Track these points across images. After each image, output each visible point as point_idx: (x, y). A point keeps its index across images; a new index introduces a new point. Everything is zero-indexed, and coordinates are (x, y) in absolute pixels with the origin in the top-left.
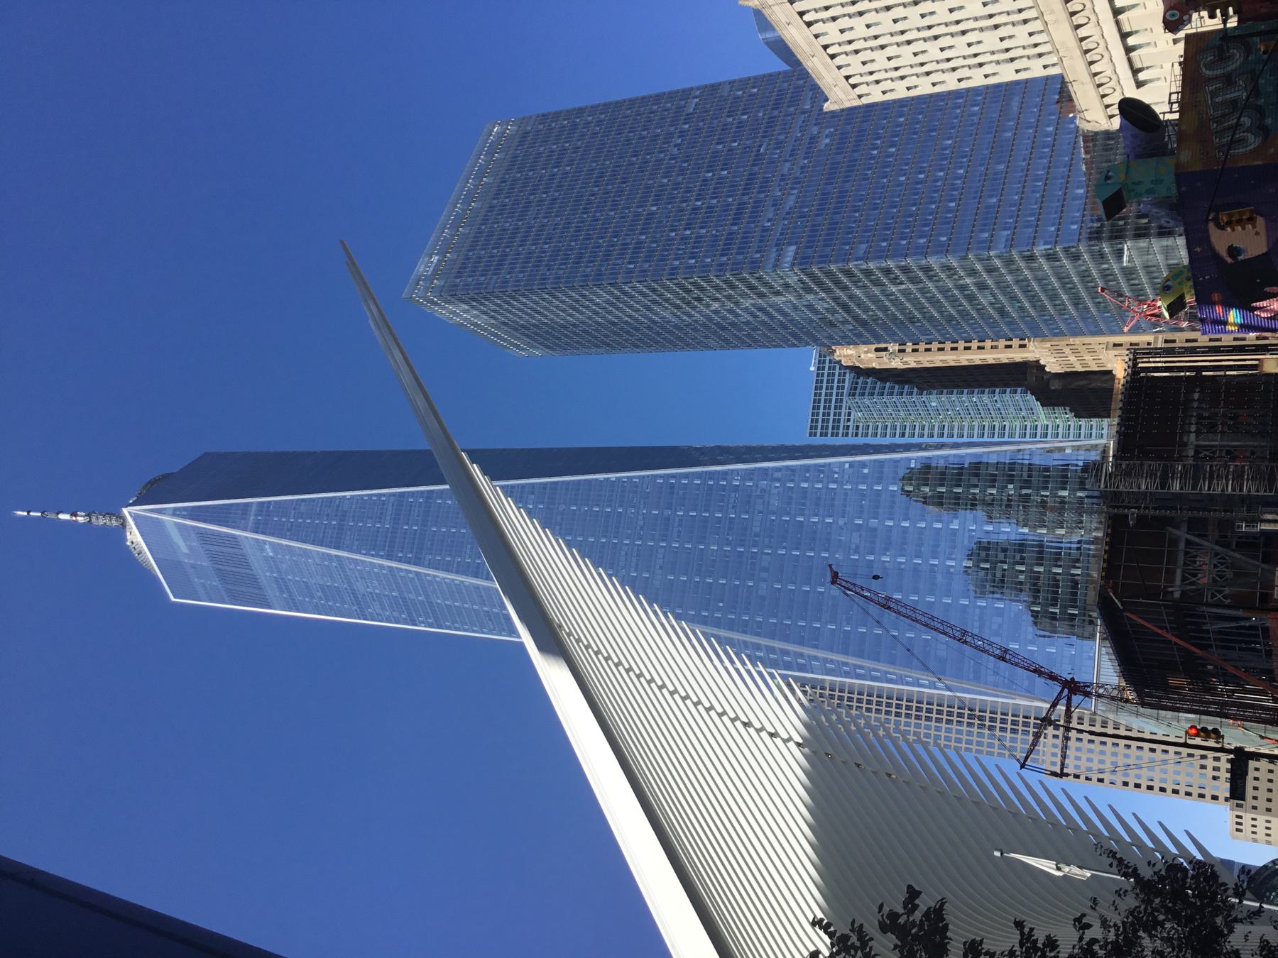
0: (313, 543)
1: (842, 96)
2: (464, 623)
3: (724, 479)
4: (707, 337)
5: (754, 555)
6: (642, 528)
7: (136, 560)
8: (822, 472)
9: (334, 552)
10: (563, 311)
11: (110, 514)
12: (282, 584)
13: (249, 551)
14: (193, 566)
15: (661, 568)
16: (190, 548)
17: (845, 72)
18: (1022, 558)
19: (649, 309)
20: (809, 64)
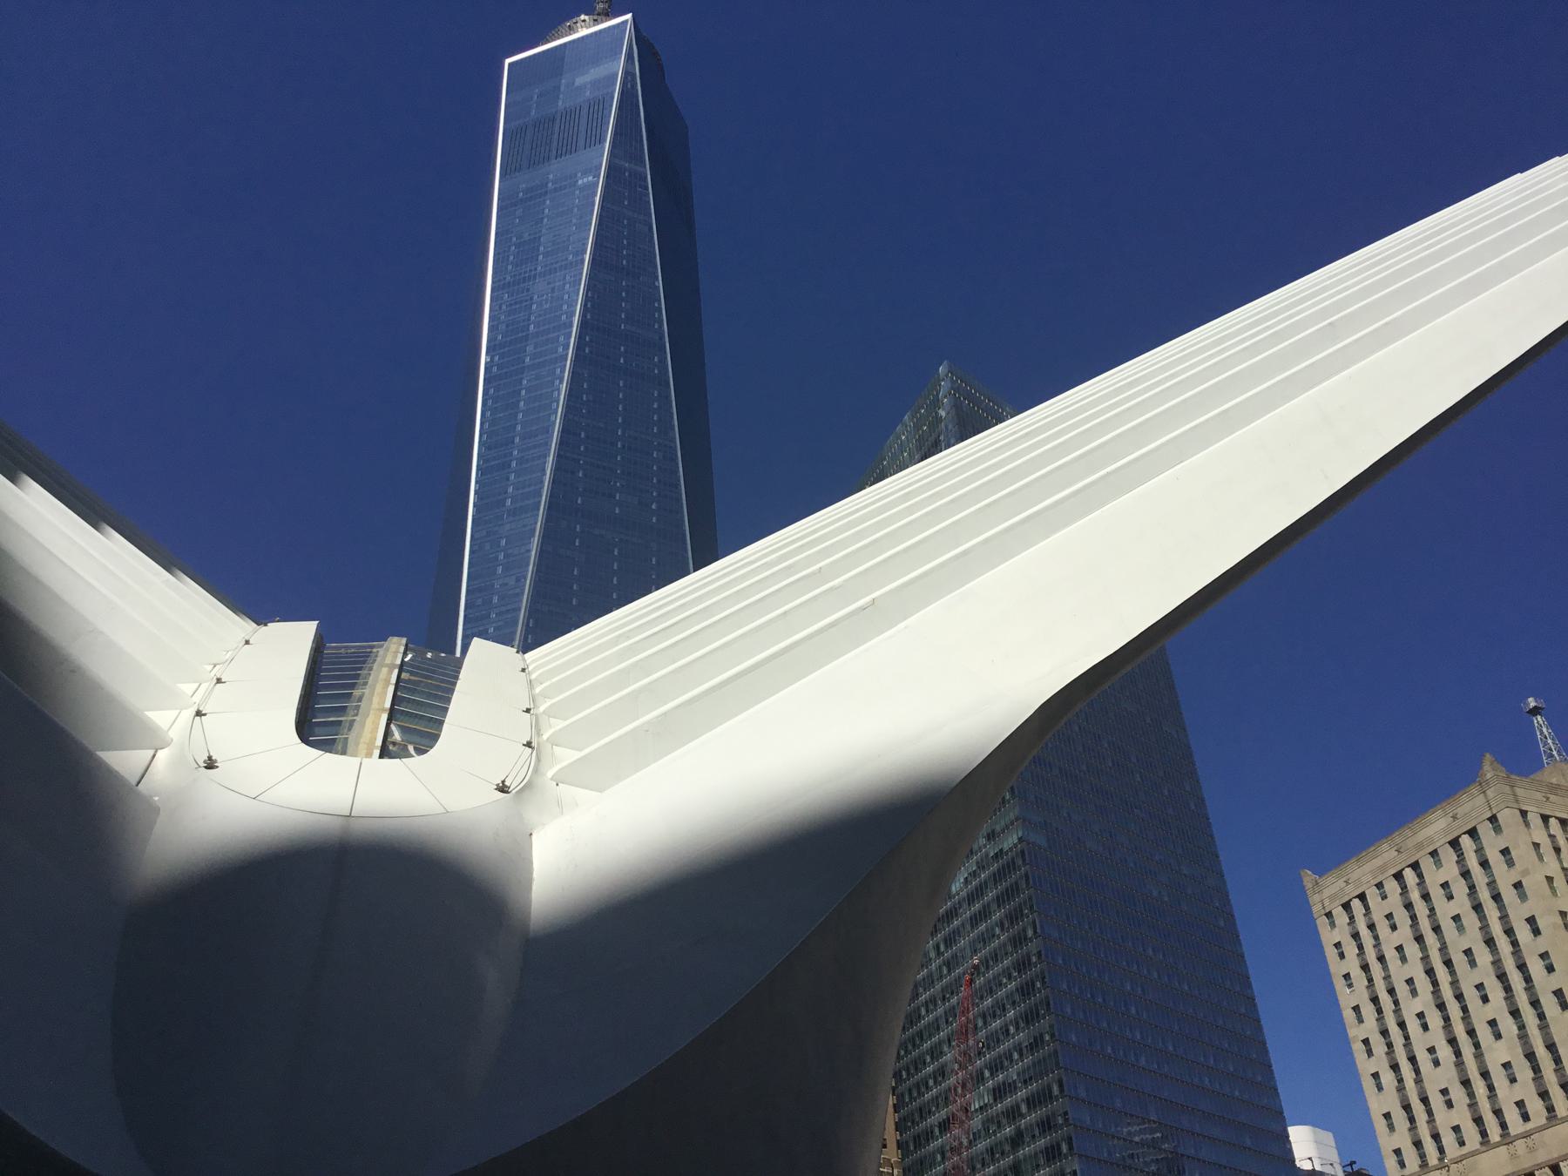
1: (1327, 893)
20: (1385, 846)
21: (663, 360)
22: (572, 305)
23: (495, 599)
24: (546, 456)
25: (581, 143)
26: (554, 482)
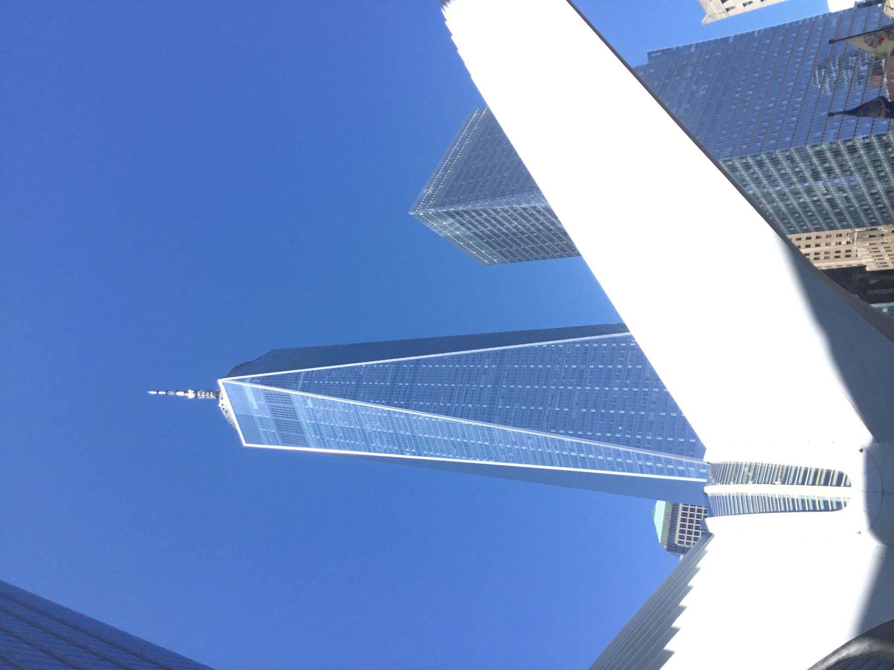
0: (339, 396)
1: (715, 11)
2: (436, 451)
3: (624, 342)
5: (645, 394)
6: (564, 378)
7: (223, 417)
9: (352, 402)
10: (516, 219)
12: (317, 428)
13: (297, 404)
14: (260, 419)
15: (577, 404)
16: (259, 405)
21: (406, 362)
22: (377, 410)
23: (540, 450)
24: (461, 424)
25: (289, 406)
26: (475, 419)
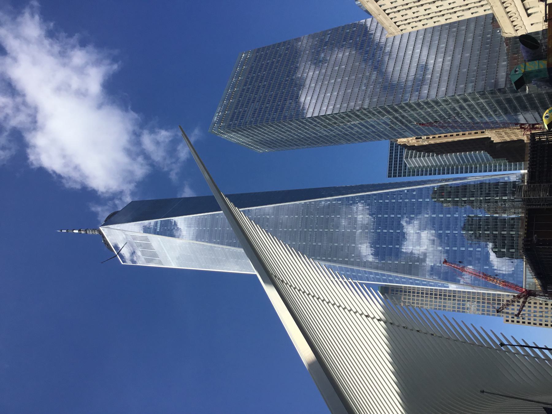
1: (394, 31)
4: (340, 139)
6: (317, 224)
8: (395, 195)
10: (277, 132)
11: (94, 230)
17: (394, 20)
18: (488, 228)
19: (314, 129)
